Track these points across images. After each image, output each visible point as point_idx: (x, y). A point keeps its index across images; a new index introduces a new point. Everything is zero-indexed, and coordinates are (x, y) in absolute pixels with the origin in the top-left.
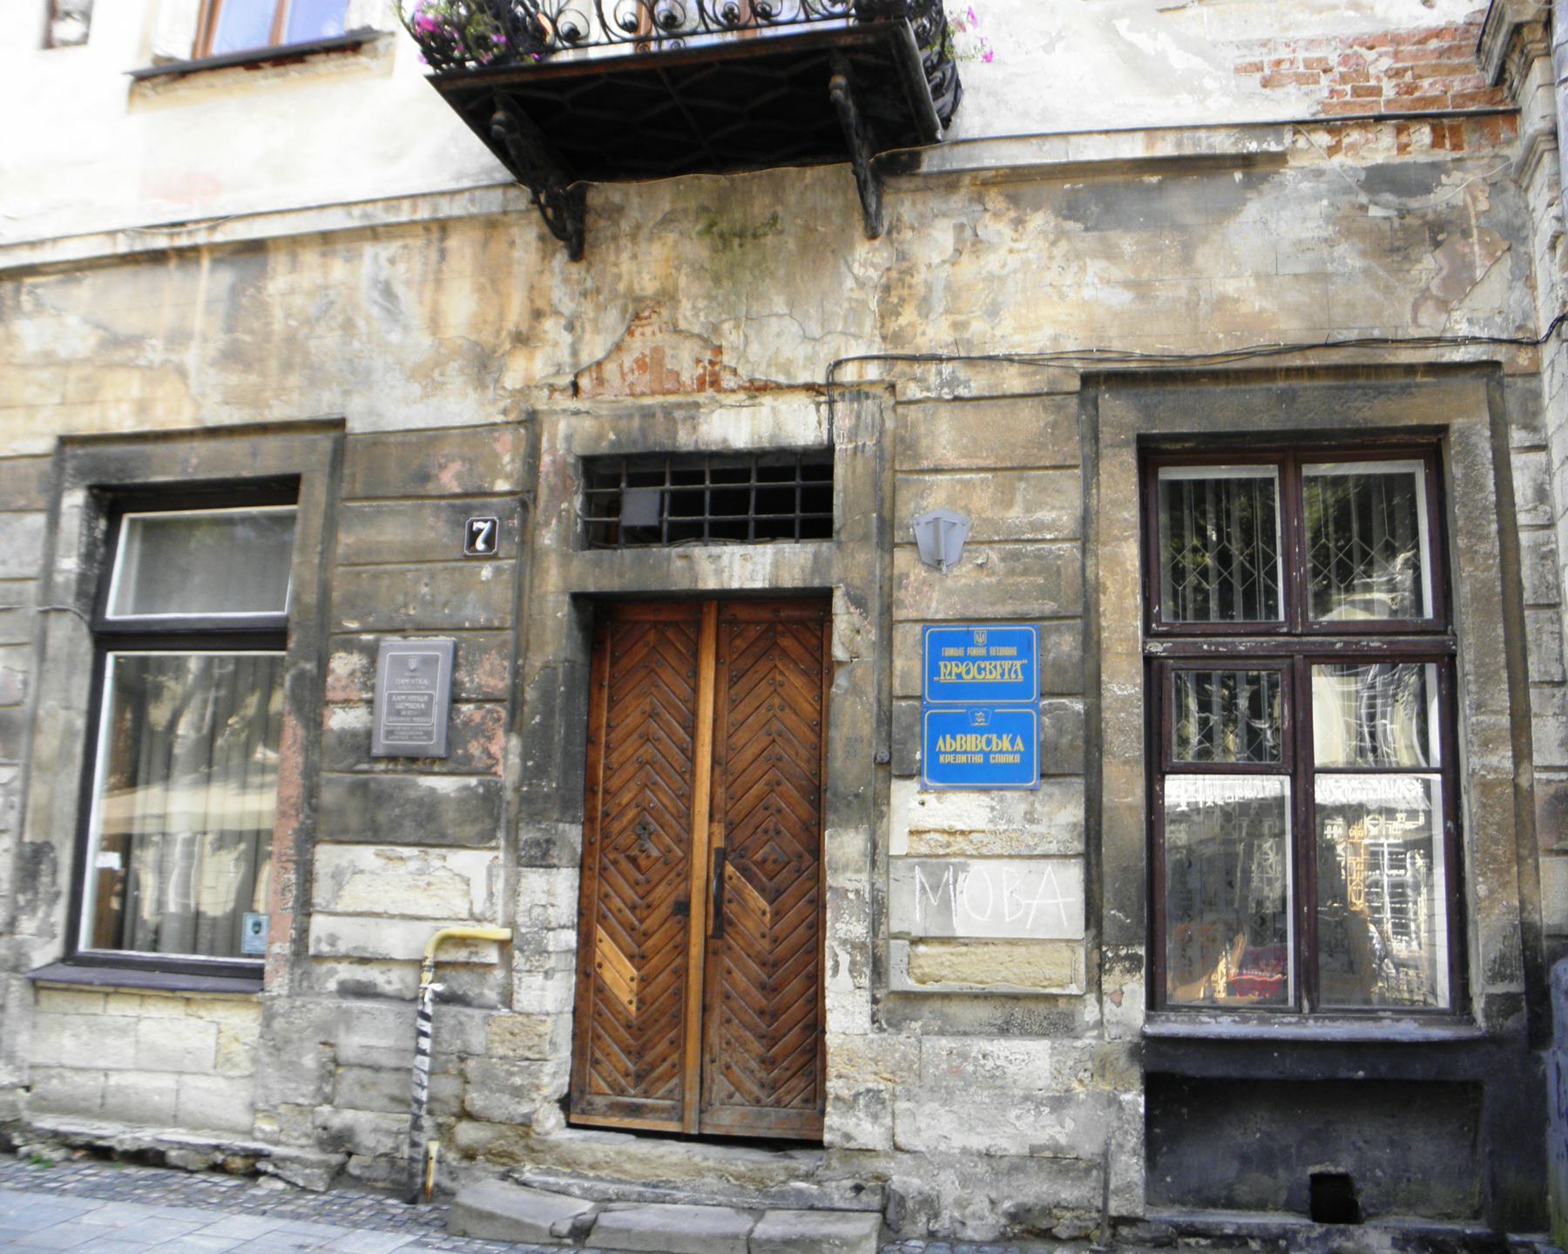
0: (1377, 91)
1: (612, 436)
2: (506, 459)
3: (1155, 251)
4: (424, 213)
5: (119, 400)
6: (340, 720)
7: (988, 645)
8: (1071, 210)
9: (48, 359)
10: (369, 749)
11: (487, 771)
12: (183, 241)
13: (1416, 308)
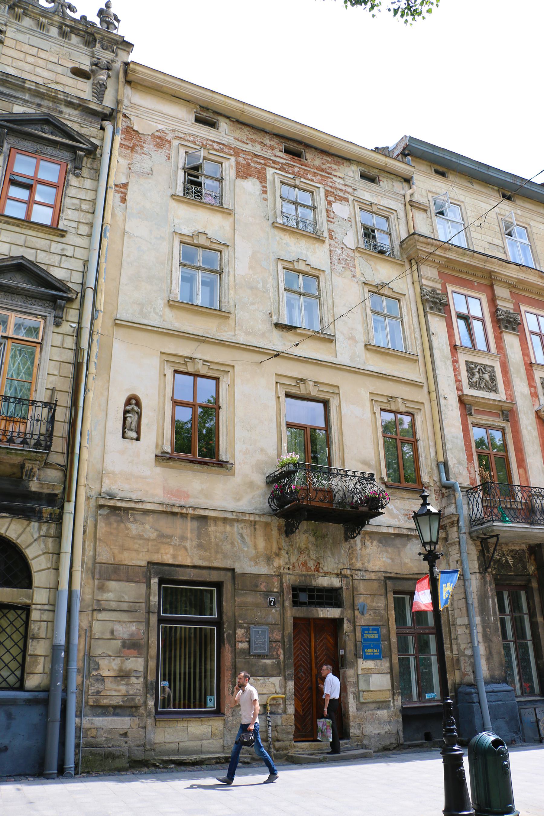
3: (394, 552)
4: (252, 518)
5: (166, 554)
8: (380, 542)
9: (141, 537)
10: (249, 653)
11: (277, 658)
12: (184, 511)
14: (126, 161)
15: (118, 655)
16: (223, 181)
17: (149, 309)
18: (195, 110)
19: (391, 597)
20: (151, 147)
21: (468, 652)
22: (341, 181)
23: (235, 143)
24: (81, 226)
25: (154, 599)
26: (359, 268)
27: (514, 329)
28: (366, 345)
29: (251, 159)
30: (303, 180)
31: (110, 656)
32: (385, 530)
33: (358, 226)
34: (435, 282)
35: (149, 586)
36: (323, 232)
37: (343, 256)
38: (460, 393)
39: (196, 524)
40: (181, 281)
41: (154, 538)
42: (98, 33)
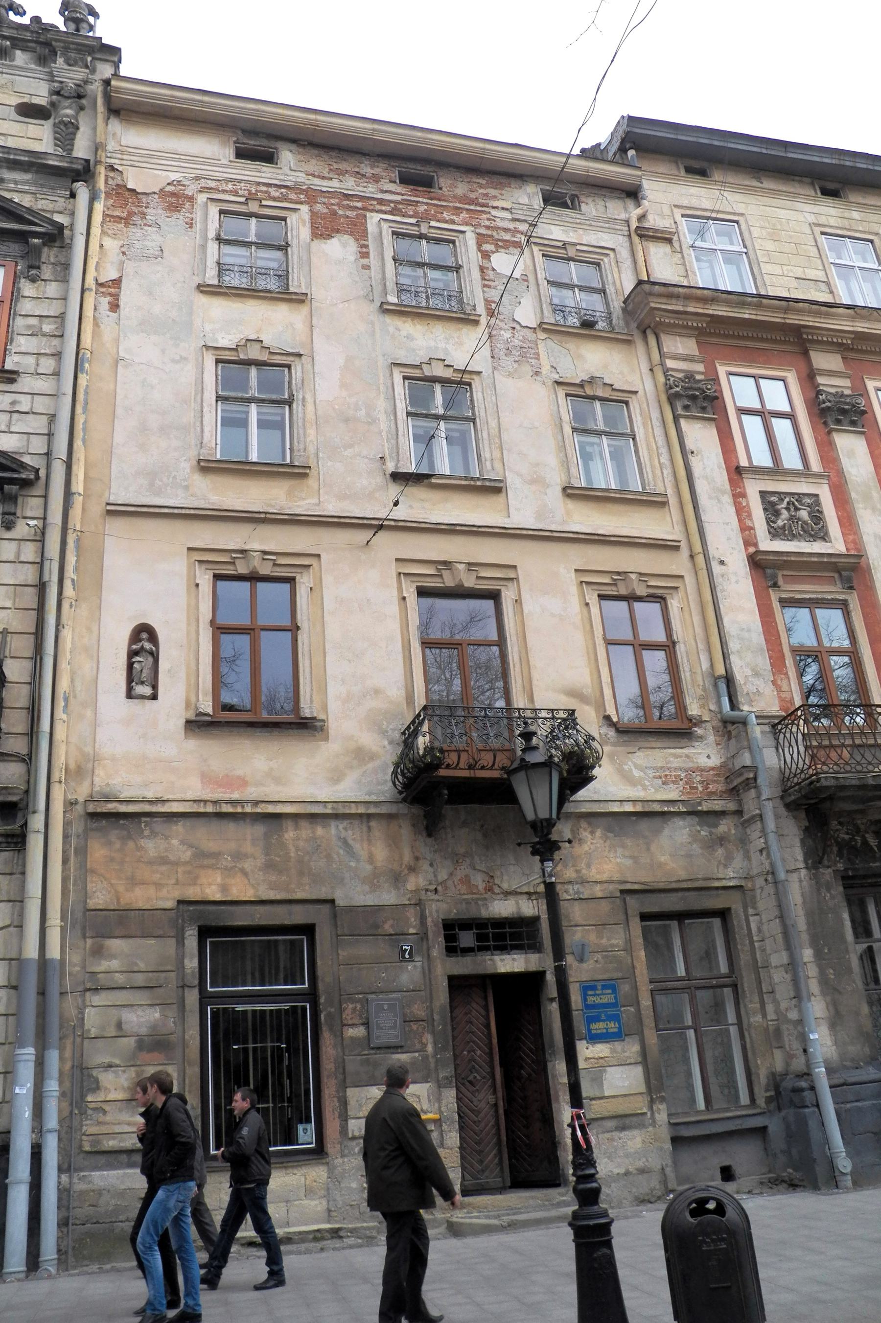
0: (696, 788)
1: (455, 911)
2: (413, 919)
5: (210, 884)
6: (351, 1032)
7: (602, 989)
8: (609, 829)
9: (163, 861)
13: (718, 867)
14: (116, 242)
15: (132, 1063)
16: (289, 249)
17: (165, 479)
18: (235, 139)
19: (636, 925)
20: (160, 211)
21: (793, 1015)
22: (508, 215)
23: (308, 182)
24: (43, 360)
25: (192, 964)
26: (546, 357)
27: (853, 423)
28: (564, 489)
29: (338, 204)
30: (433, 223)
31: (117, 1066)
32: (616, 808)
33: (541, 287)
34: (691, 361)
35: (181, 941)
36: (475, 306)
37: (516, 342)
38: (752, 550)
39: (259, 829)
40: (222, 425)
41: (188, 859)
42: (57, 40)
